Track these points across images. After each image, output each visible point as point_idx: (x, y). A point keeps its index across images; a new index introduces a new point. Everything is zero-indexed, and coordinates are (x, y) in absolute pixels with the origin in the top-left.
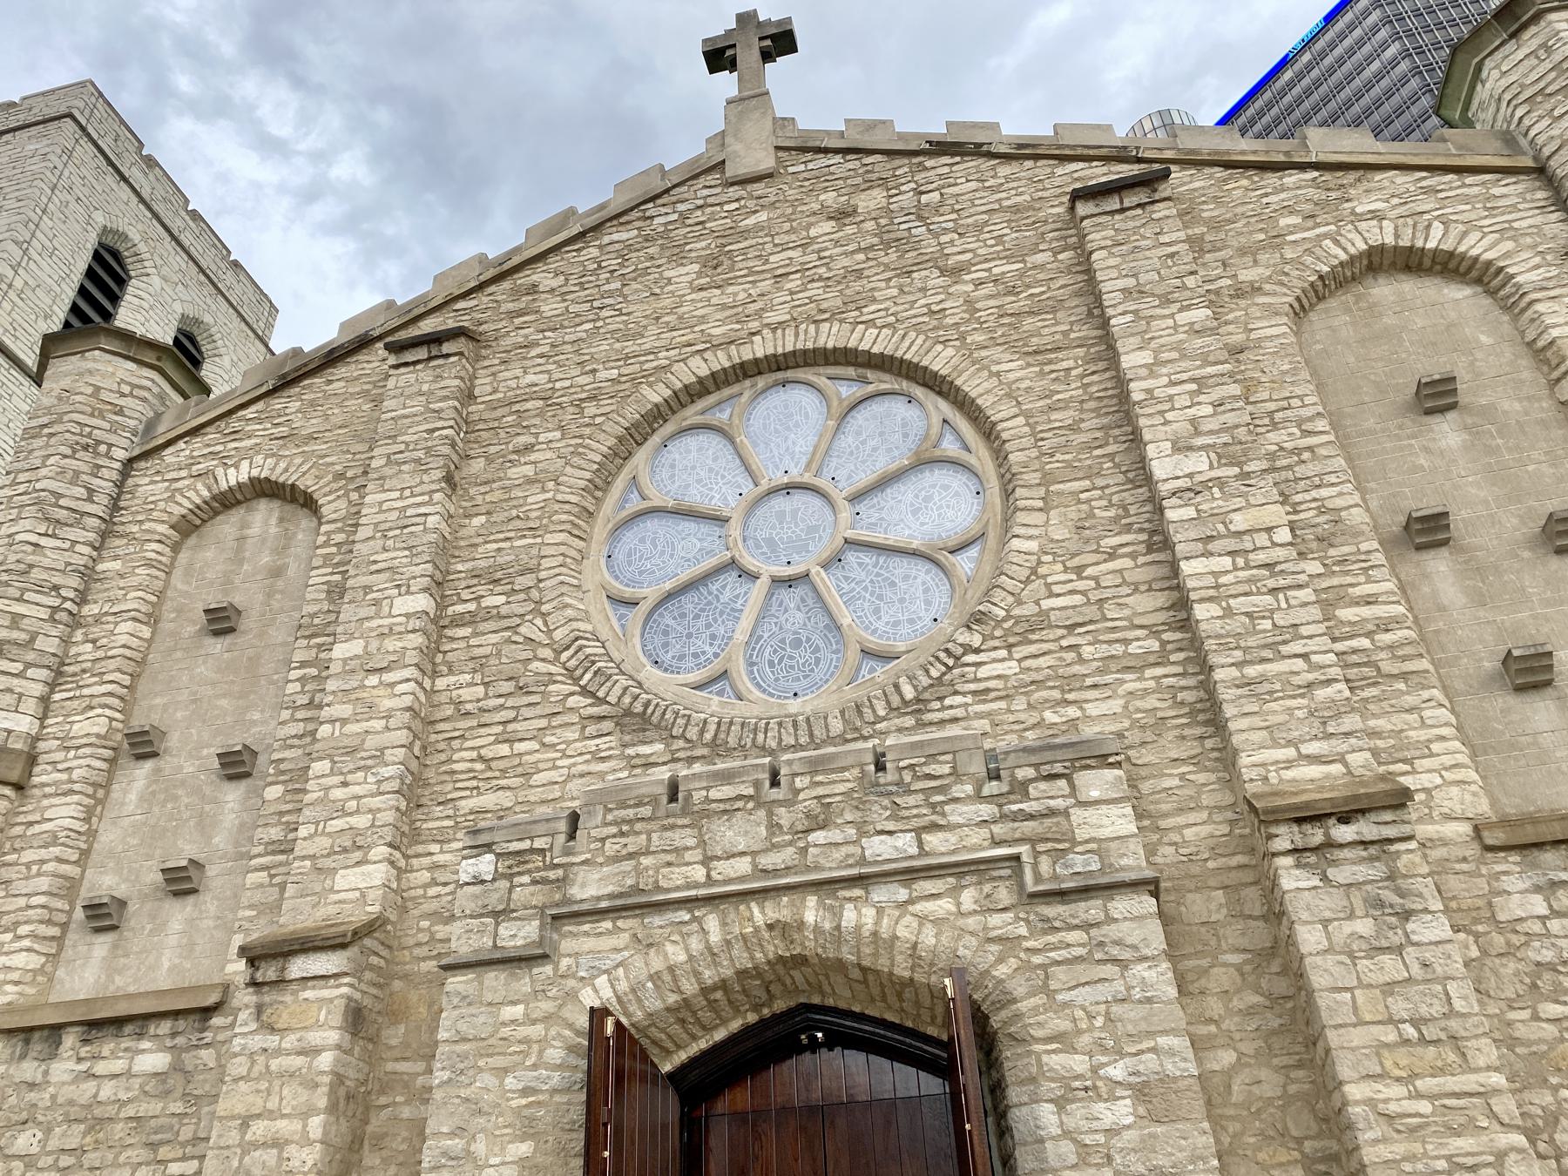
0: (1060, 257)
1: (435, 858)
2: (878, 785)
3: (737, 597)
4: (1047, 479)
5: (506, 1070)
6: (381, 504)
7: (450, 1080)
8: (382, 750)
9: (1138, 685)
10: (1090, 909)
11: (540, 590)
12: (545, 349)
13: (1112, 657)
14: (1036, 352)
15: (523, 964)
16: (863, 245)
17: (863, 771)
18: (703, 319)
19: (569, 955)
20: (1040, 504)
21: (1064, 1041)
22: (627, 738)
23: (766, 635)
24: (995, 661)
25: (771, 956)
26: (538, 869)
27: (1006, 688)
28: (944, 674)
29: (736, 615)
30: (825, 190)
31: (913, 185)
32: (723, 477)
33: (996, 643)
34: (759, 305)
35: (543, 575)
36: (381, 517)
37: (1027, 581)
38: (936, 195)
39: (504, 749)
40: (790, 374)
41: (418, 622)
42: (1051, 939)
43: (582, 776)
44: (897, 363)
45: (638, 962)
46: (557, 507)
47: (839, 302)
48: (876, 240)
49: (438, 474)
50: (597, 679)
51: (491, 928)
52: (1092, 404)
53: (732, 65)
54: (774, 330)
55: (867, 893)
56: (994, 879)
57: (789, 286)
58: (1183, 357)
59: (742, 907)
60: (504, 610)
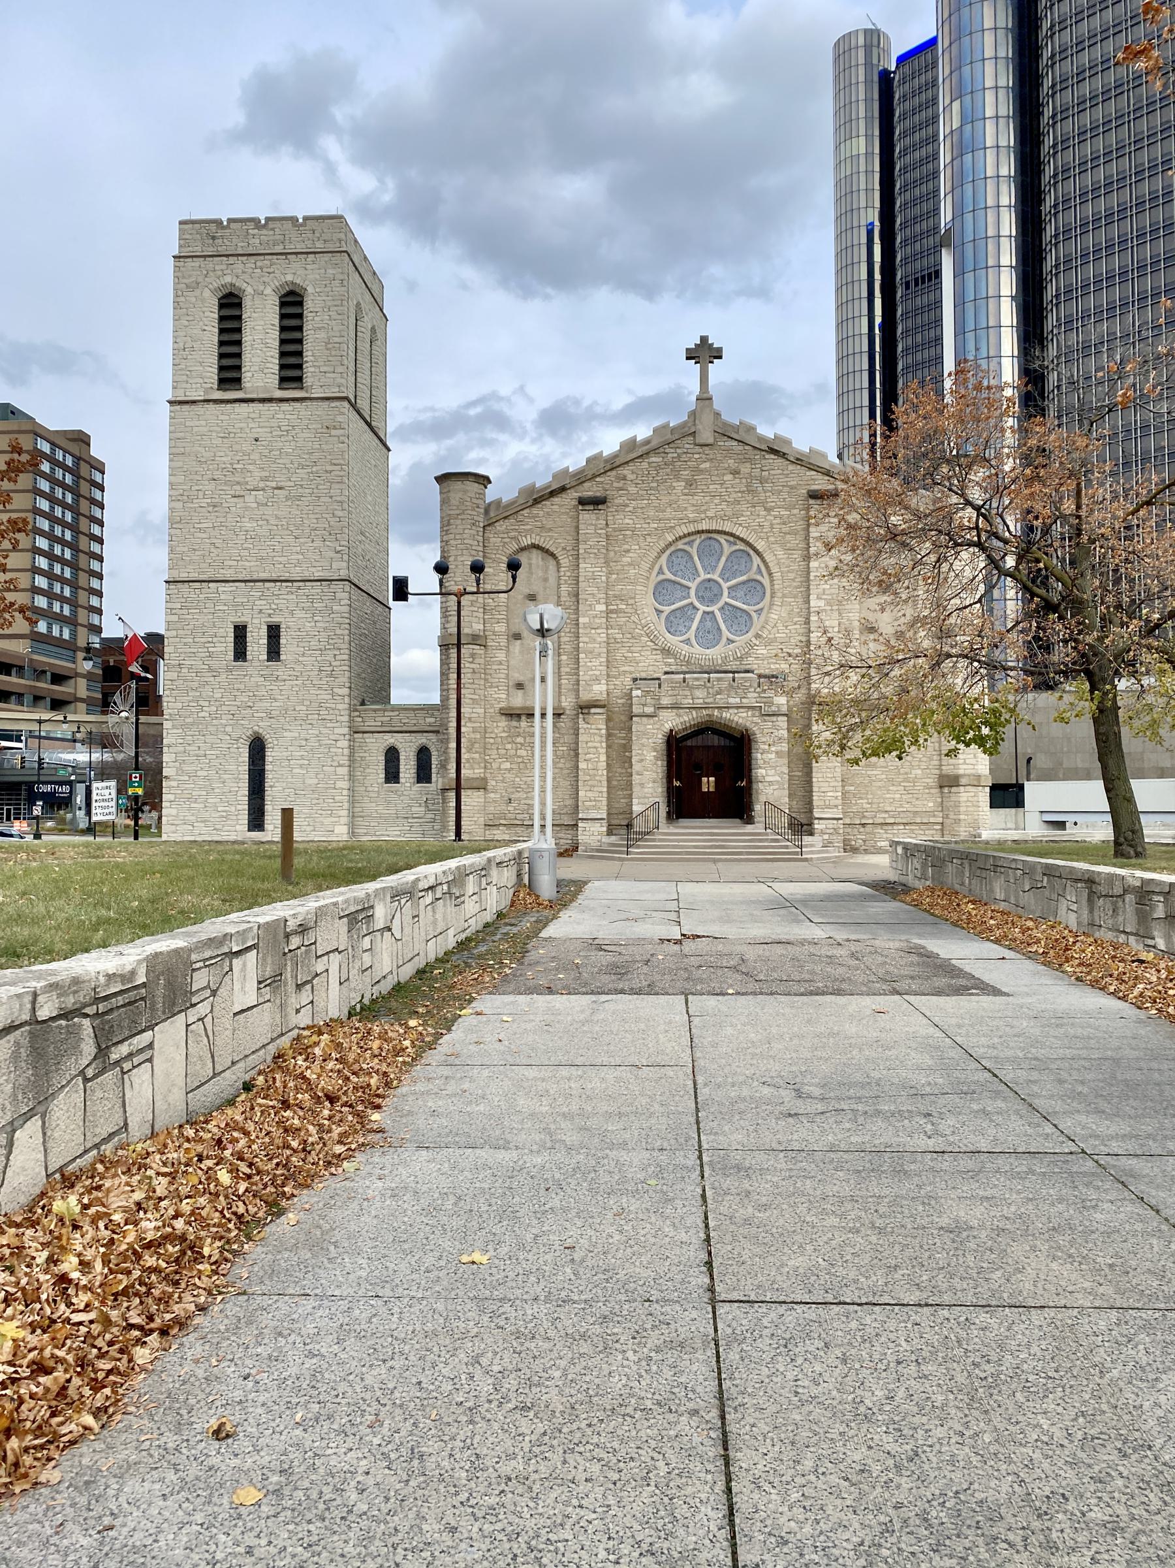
4: (784, 596)
10: (774, 719)
29: (692, 620)
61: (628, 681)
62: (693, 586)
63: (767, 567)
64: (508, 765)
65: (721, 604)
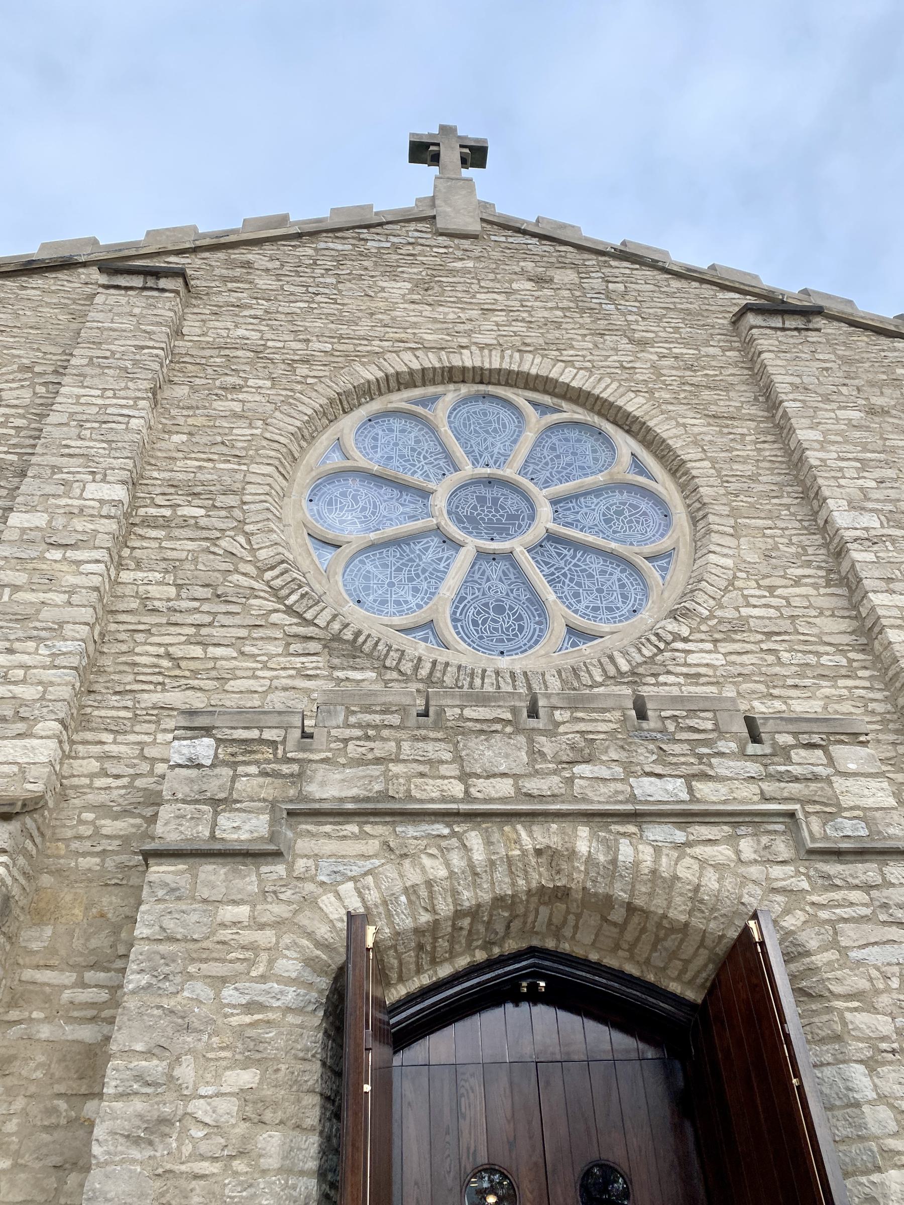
0: (728, 353)
1: (106, 748)
2: (641, 729)
3: (440, 559)
4: (734, 513)
5: (224, 980)
6: (78, 397)
7: (150, 985)
8: (61, 625)
9: (833, 691)
10: (867, 871)
11: (244, 512)
12: (260, 313)
13: (807, 664)
14: (714, 416)
15: (249, 860)
16: (560, 305)
17: (624, 715)
18: (415, 325)
19: (307, 857)
20: (731, 531)
21: (864, 1000)
22: (336, 661)
23: (469, 598)
24: (702, 651)
25: (534, 884)
26: (268, 762)
27: (715, 676)
28: (656, 655)
30: (524, 259)
31: (600, 275)
32: (425, 458)
33: (703, 636)
34: (468, 327)
35: (247, 498)
36: (79, 409)
37: (726, 590)
38: (621, 287)
39: (197, 651)
40: (491, 389)
41: (113, 510)
42: (837, 895)
43: (285, 689)
44: (592, 400)
45: (390, 871)
46: (265, 443)
47: (541, 341)
48: (572, 305)
49: (147, 385)
50: (305, 601)
51: (209, 816)
52: (766, 465)
53: (435, 159)
54: (482, 349)
55: (641, 830)
56: (769, 832)
57: (495, 319)
58: (846, 442)
59: (507, 829)
60: (203, 522)
65: (535, 533)
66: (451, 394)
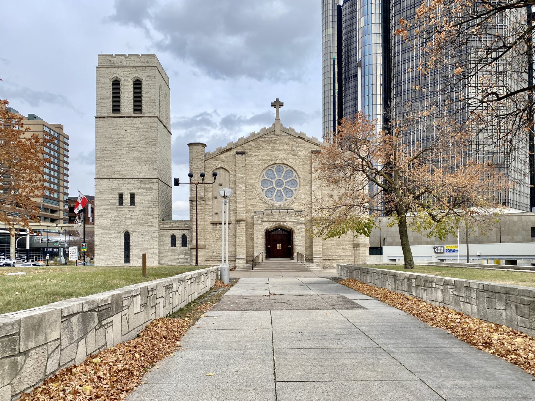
4: (304, 185)
61: (253, 213)
62: (274, 181)
63: (298, 176)
64: (213, 240)
65: (283, 187)
66: (276, 166)
